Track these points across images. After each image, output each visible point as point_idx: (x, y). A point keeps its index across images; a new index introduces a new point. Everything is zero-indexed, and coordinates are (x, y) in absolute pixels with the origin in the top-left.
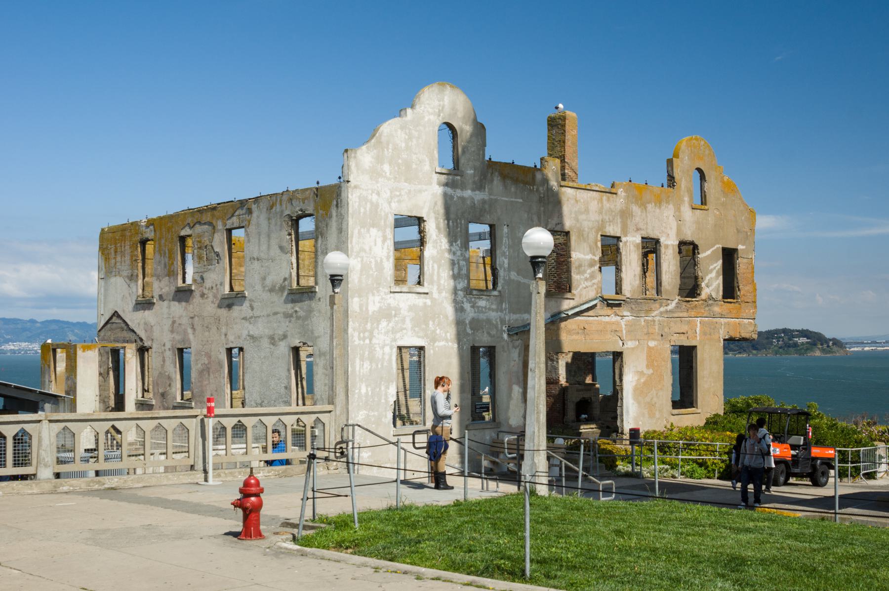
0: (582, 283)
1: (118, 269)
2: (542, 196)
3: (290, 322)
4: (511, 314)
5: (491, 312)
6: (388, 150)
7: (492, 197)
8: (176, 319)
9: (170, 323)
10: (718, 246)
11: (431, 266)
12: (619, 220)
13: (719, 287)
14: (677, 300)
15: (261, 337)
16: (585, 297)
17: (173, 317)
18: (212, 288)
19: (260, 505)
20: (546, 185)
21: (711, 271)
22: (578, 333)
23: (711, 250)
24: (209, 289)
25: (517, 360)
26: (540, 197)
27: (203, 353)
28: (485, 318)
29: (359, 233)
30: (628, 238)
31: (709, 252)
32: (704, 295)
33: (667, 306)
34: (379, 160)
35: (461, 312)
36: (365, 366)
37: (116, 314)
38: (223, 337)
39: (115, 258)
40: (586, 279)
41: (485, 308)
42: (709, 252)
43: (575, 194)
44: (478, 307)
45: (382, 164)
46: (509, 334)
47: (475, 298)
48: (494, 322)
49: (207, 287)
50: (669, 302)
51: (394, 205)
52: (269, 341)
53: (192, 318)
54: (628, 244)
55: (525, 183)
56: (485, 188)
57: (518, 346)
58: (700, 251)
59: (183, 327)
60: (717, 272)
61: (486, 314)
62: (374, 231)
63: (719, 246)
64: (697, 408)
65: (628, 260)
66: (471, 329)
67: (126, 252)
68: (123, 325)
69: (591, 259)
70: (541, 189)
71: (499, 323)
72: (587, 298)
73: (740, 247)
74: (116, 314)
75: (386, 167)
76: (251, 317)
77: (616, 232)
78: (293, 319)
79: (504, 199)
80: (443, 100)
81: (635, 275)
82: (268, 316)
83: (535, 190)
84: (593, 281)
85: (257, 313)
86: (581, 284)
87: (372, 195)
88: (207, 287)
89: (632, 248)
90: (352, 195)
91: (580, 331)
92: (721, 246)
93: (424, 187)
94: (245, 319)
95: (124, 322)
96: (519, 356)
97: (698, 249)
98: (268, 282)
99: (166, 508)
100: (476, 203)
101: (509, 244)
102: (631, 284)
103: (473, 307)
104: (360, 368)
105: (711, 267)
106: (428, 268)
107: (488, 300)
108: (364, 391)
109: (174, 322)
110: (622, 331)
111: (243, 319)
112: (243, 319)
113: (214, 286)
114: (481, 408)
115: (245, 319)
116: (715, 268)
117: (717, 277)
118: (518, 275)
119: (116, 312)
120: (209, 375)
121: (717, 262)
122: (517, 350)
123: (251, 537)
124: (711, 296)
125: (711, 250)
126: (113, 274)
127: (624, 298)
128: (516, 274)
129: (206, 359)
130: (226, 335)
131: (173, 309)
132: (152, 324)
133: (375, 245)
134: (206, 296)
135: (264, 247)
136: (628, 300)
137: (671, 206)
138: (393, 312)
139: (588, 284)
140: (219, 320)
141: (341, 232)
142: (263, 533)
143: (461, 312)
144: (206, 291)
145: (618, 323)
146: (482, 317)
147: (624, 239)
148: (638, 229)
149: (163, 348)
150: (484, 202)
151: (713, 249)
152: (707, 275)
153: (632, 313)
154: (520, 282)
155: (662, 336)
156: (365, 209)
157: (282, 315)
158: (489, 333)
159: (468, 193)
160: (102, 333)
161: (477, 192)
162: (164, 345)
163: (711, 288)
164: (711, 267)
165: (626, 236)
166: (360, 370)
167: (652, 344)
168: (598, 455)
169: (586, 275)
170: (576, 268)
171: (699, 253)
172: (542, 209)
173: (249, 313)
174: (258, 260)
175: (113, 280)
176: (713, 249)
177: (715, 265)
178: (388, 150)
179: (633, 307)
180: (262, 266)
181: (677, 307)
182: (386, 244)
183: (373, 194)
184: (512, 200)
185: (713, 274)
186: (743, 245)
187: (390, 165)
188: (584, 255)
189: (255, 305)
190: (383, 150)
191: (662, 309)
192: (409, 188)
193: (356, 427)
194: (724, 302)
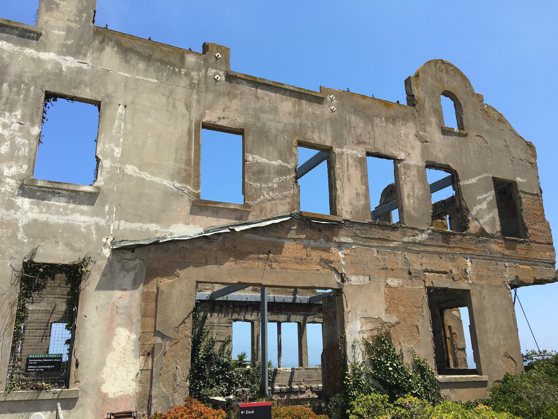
2: (196, 82)
10: (486, 175)
16: (271, 211)
21: (480, 202)
23: (477, 178)
30: (344, 150)
31: (473, 180)
54: (345, 157)
60: (489, 204)
65: (346, 175)
70: (194, 74)
73: (519, 180)
77: (324, 141)
84: (284, 193)
92: (491, 176)
100: (64, 69)
114: (39, 364)
116: (485, 199)
117: (490, 209)
125: (477, 178)
139: (277, 194)
151: (480, 177)
165: (341, 147)
176: (480, 177)
184: (137, 77)
188: (268, 159)
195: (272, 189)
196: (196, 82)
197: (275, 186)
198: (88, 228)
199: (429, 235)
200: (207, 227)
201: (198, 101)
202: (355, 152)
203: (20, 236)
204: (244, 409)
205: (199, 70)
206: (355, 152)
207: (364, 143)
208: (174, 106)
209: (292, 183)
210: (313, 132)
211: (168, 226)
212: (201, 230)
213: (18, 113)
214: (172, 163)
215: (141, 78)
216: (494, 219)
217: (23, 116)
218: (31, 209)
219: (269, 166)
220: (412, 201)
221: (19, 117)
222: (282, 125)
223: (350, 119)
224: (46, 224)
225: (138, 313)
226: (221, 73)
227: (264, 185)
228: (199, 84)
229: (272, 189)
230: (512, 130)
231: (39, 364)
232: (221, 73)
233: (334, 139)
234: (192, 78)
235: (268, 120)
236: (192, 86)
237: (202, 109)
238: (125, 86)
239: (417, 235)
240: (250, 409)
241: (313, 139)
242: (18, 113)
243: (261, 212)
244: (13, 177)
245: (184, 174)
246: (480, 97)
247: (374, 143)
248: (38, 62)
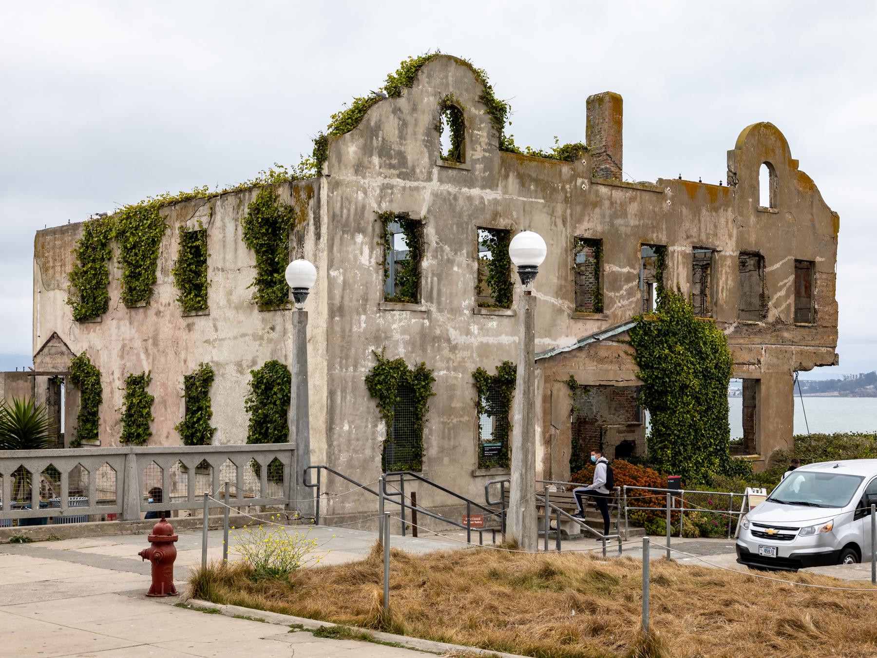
0: (617, 301)
1: (57, 281)
2: (569, 195)
3: (260, 345)
5: (503, 336)
6: (377, 140)
7: (507, 196)
8: (127, 342)
9: (120, 346)
10: (789, 258)
11: (429, 279)
15: (227, 364)
16: (621, 318)
17: (123, 340)
18: (169, 304)
19: (173, 557)
20: (574, 183)
21: (780, 289)
22: (612, 362)
23: (781, 263)
24: (165, 306)
26: (566, 197)
27: (158, 383)
28: (496, 342)
29: (341, 239)
30: (676, 248)
31: (777, 266)
32: (771, 319)
34: (367, 150)
35: (467, 335)
36: (348, 398)
37: (54, 336)
38: (183, 363)
39: (53, 267)
42: (777, 266)
43: (610, 193)
45: (371, 156)
49: (164, 303)
50: (726, 325)
51: (384, 205)
52: (236, 368)
53: (145, 340)
54: (676, 255)
56: (498, 186)
58: (766, 264)
59: (135, 352)
60: (788, 290)
62: (359, 238)
64: (760, 454)
65: (675, 274)
67: (67, 259)
68: (64, 349)
69: (629, 272)
70: (568, 186)
71: (513, 349)
73: (818, 259)
74: (54, 336)
75: (376, 160)
76: (215, 340)
77: (661, 240)
78: (264, 342)
79: (521, 198)
80: (447, 77)
82: (235, 338)
84: (631, 300)
85: (222, 334)
86: (615, 303)
87: (357, 193)
88: (164, 303)
90: (333, 193)
91: (614, 360)
92: (794, 258)
93: (422, 184)
94: (206, 341)
95: (65, 344)
97: (764, 262)
98: (235, 298)
99: (74, 562)
104: (341, 401)
105: (781, 284)
106: (427, 282)
108: (346, 427)
109: (124, 346)
111: (204, 342)
112: (204, 342)
113: (171, 302)
114: (490, 450)
115: (206, 341)
116: (786, 284)
117: (787, 296)
119: (55, 333)
120: (166, 409)
123: (160, 593)
124: (780, 319)
125: (781, 263)
126: (52, 286)
129: (162, 390)
130: (185, 361)
131: (123, 329)
132: (99, 348)
133: (362, 254)
134: (161, 314)
135: (230, 256)
138: (383, 335)
139: (626, 302)
140: (178, 343)
141: (319, 238)
142: (177, 589)
143: (467, 335)
144: (162, 309)
147: (671, 249)
149: (111, 377)
150: (496, 202)
151: (784, 261)
156: (349, 210)
157: (251, 337)
159: (476, 192)
160: (38, 360)
161: (488, 191)
162: (113, 374)
163: (780, 309)
164: (781, 284)
165: (673, 245)
166: (341, 403)
168: (627, 508)
169: (621, 292)
171: (765, 267)
172: (569, 211)
173: (212, 335)
174: (223, 270)
175: (51, 294)
176: (784, 261)
177: (786, 281)
178: (377, 140)
180: (228, 279)
181: (736, 332)
182: (375, 252)
183: (359, 192)
184: (531, 200)
185: (782, 293)
186: (822, 257)
187: (380, 157)
188: (620, 267)
189: (220, 325)
190: (372, 139)
192: (403, 185)
193: (322, 470)
194: (795, 325)
195: (622, 297)
196: (569, 195)
197: (625, 293)
198: (509, 345)
199: (735, 328)
200: (580, 337)
201: (571, 215)
202: (683, 248)
203: (475, 355)
204: (670, 479)
205: (571, 182)
206: (683, 248)
207: (692, 236)
208: (556, 225)
209: (636, 288)
210: (653, 232)
211: (555, 340)
212: (575, 341)
213: (465, 251)
214: (556, 281)
215: (533, 200)
216: (789, 305)
217: (468, 253)
218: (479, 333)
219: (620, 274)
220: (724, 295)
221: (465, 255)
222: (630, 228)
223: (681, 211)
224: (487, 345)
226: (586, 181)
227: (617, 294)
228: (571, 196)
229: (622, 297)
230: (821, 200)
231: (490, 450)
232: (586, 181)
233: (668, 237)
234: (566, 192)
235: (621, 225)
236: (566, 200)
237: (574, 223)
238: (524, 211)
239: (725, 329)
240: (672, 479)
241: (653, 240)
242: (465, 251)
243: (614, 320)
244: (467, 309)
245: (564, 290)
246: (795, 163)
247: (699, 235)
248: (470, 198)
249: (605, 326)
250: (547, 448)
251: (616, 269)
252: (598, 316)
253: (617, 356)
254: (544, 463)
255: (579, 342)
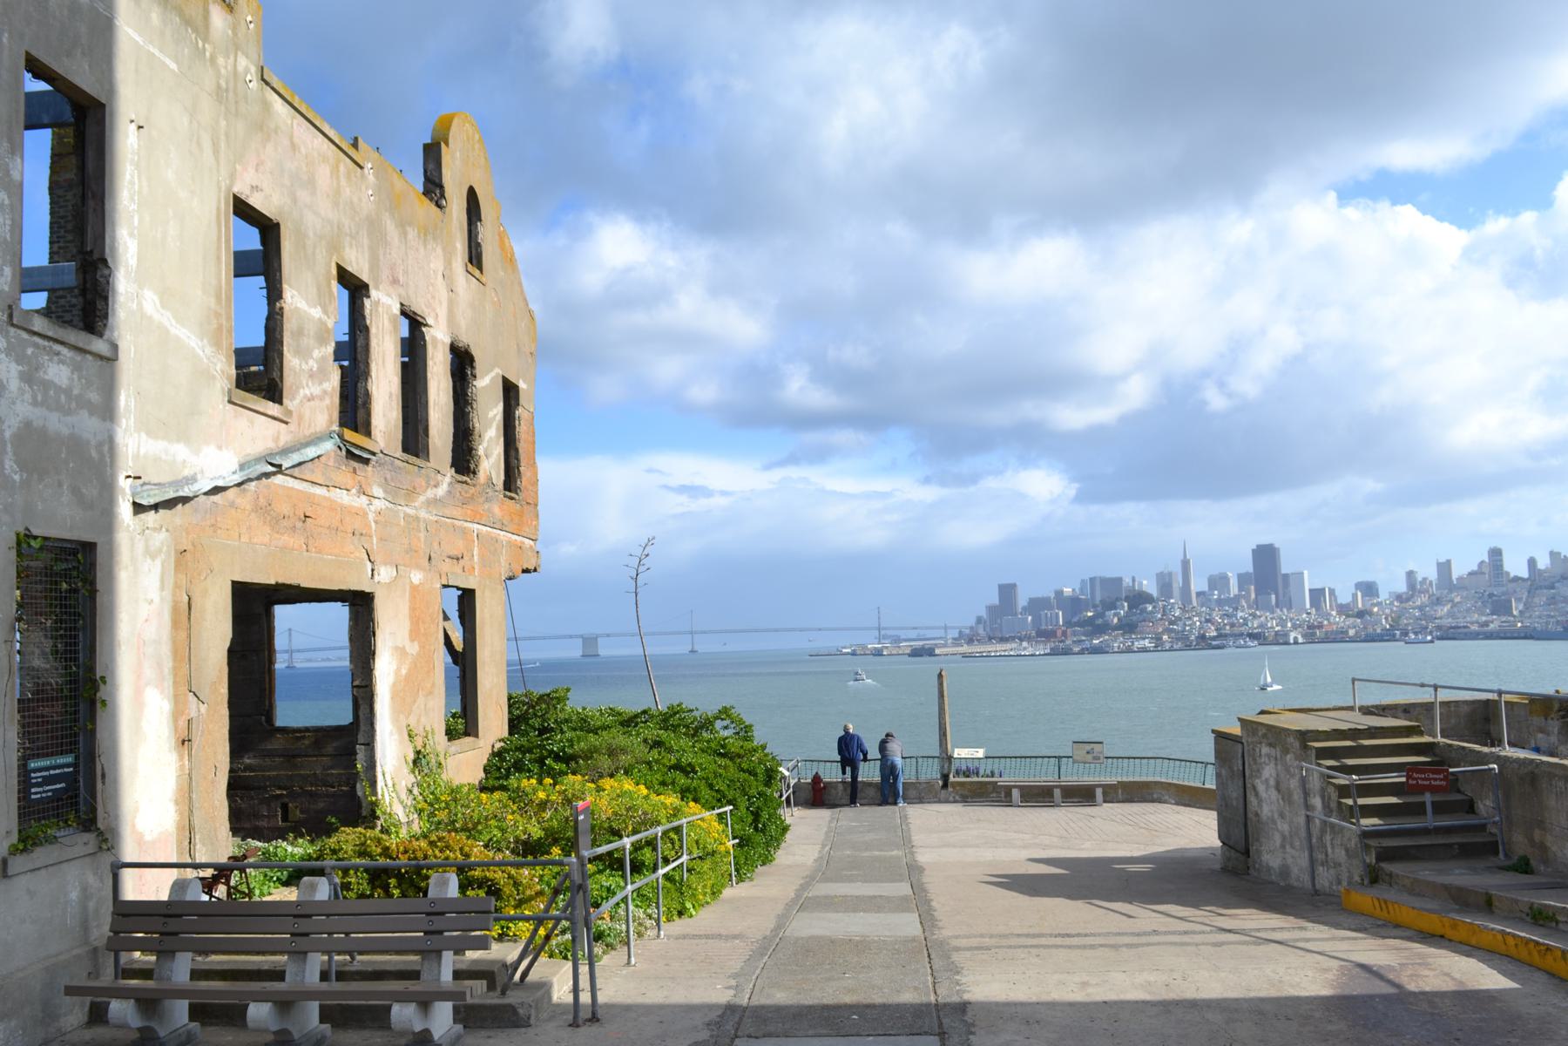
0: (304, 382)
4: (143, 435)
5: (85, 414)
12: (366, 242)
13: (500, 459)
14: (449, 475)
25: (157, 600)
28: (65, 431)
33: (435, 486)
40: (312, 375)
41: (68, 392)
44: (47, 385)
46: (135, 504)
47: (36, 346)
48: (94, 454)
50: (439, 477)
55: (188, 22)
57: (160, 551)
58: (478, 372)
60: (497, 429)
61: (69, 419)
63: (497, 372)
66: (22, 465)
69: (320, 319)
72: (312, 430)
81: (391, 394)
83: (208, 54)
89: (386, 323)
91: (299, 524)
96: (162, 588)
97: (473, 367)
101: (140, 192)
102: (384, 416)
103: (28, 378)
105: (491, 414)
107: (76, 368)
110: (371, 537)
114: (48, 781)
116: (495, 415)
117: (498, 437)
118: (163, 306)
121: (497, 405)
122: (158, 562)
127: (376, 450)
128: (156, 298)
136: (381, 455)
137: (439, 250)
145: (360, 514)
146: (55, 423)
147: (373, 292)
148: (395, 281)
151: (493, 374)
152: (486, 431)
153: (385, 491)
154: (167, 331)
155: (430, 559)
158: (75, 491)
165: (377, 288)
167: (416, 577)
170: (292, 333)
176: (493, 374)
177: (495, 411)
179: (388, 477)
181: (449, 492)
191: (430, 493)
194: (505, 496)
225: (169, 654)
231: (48, 781)
249: (285, 435)
250: (181, 758)
251: (302, 304)
252: (272, 408)
253: (302, 517)
254: (177, 803)
255: (242, 467)
